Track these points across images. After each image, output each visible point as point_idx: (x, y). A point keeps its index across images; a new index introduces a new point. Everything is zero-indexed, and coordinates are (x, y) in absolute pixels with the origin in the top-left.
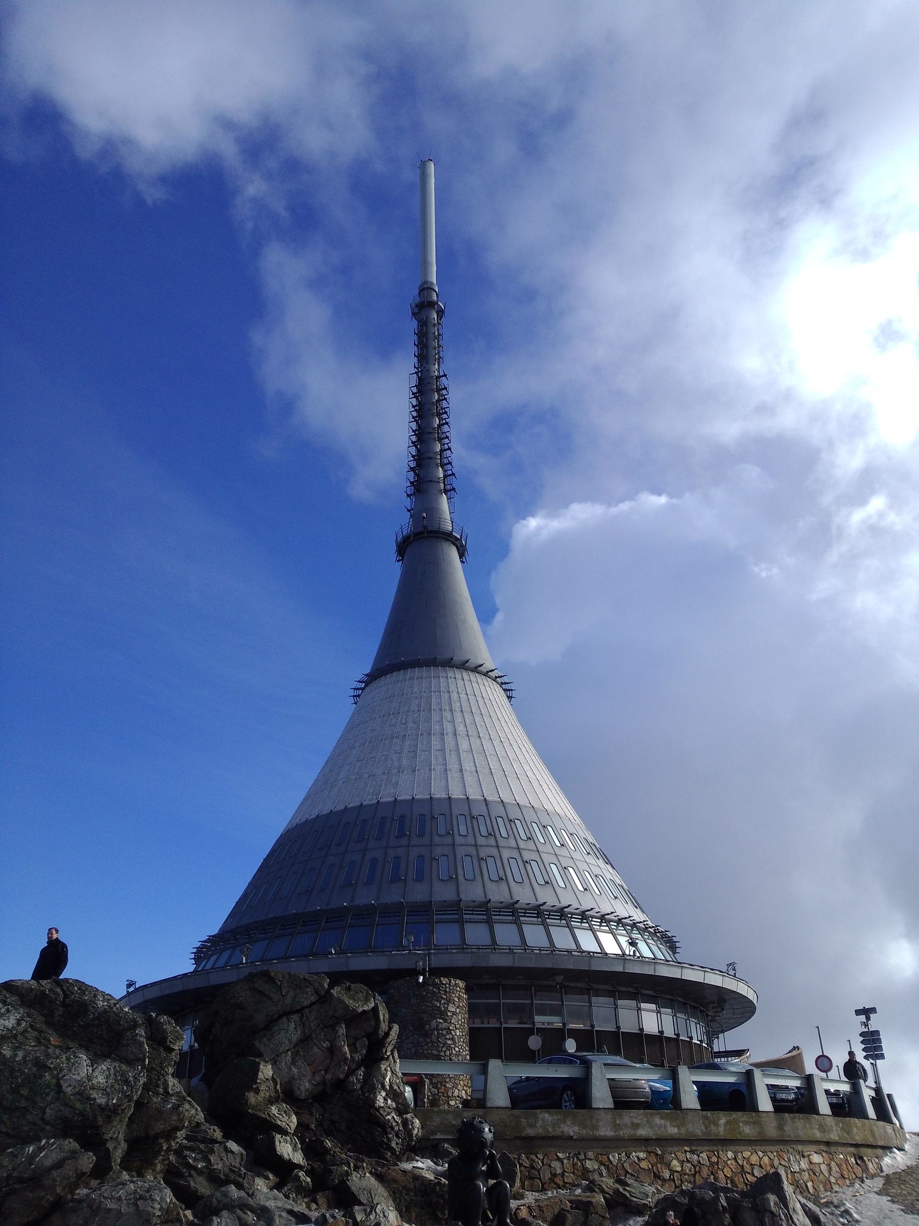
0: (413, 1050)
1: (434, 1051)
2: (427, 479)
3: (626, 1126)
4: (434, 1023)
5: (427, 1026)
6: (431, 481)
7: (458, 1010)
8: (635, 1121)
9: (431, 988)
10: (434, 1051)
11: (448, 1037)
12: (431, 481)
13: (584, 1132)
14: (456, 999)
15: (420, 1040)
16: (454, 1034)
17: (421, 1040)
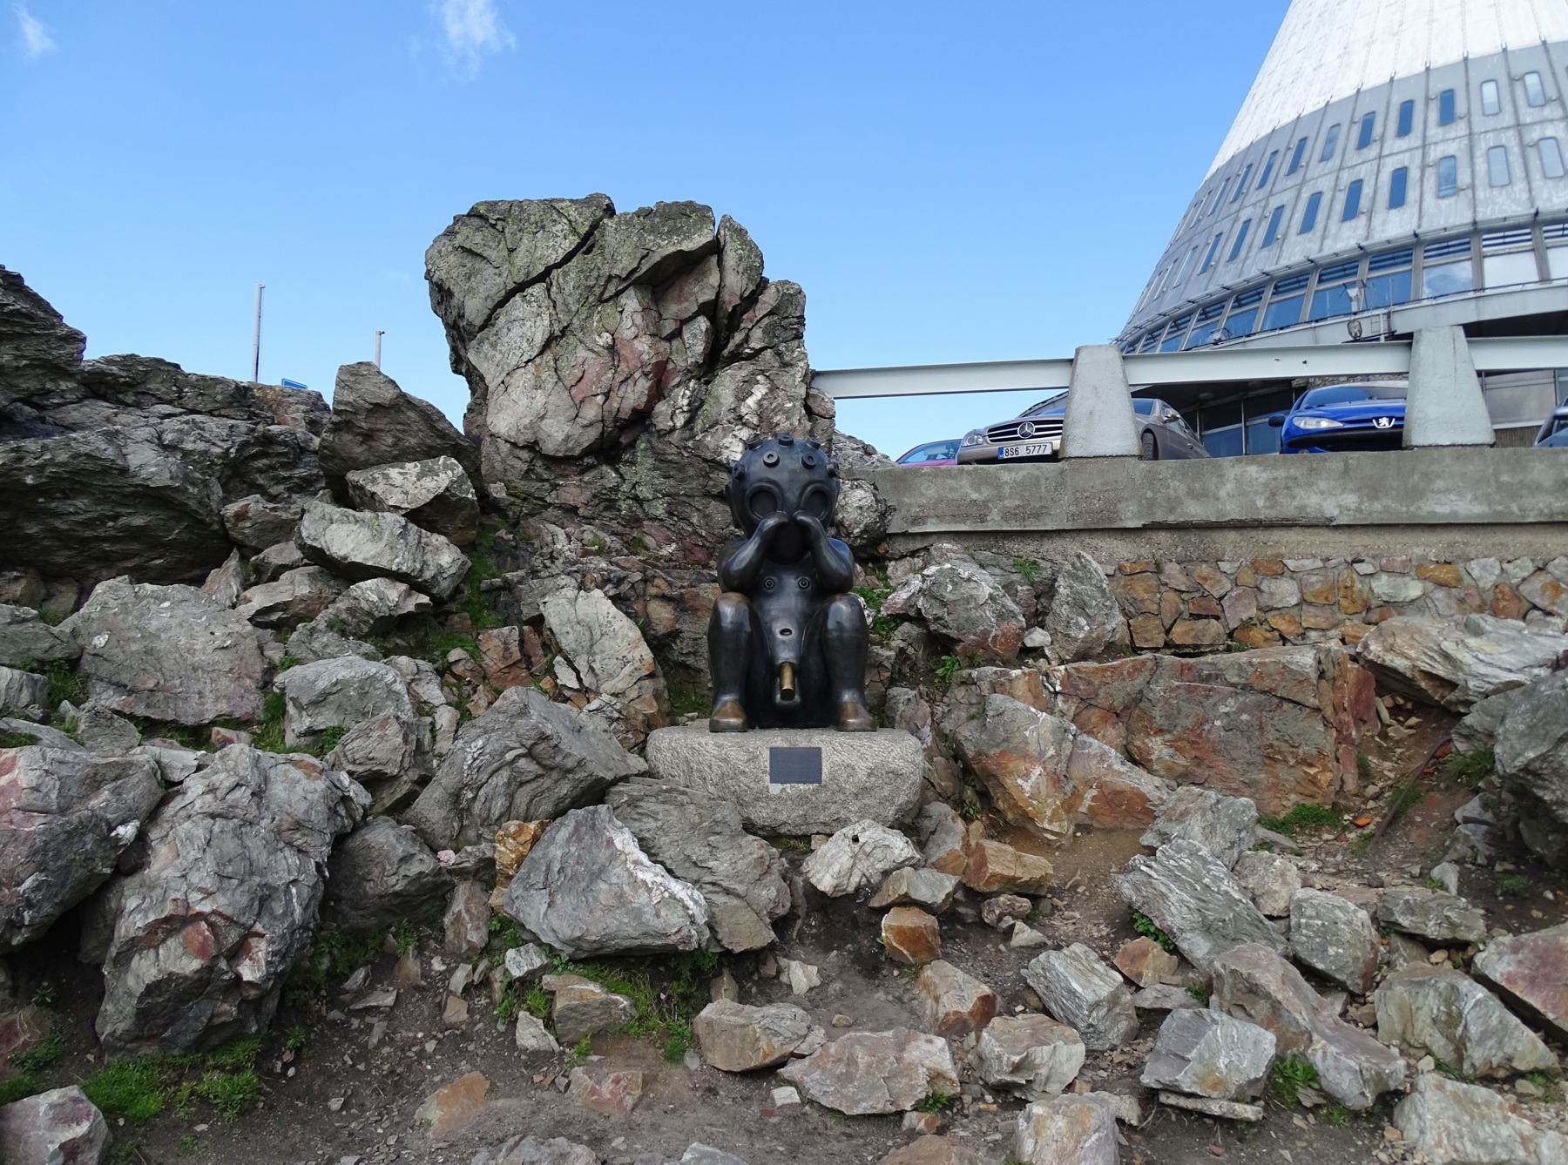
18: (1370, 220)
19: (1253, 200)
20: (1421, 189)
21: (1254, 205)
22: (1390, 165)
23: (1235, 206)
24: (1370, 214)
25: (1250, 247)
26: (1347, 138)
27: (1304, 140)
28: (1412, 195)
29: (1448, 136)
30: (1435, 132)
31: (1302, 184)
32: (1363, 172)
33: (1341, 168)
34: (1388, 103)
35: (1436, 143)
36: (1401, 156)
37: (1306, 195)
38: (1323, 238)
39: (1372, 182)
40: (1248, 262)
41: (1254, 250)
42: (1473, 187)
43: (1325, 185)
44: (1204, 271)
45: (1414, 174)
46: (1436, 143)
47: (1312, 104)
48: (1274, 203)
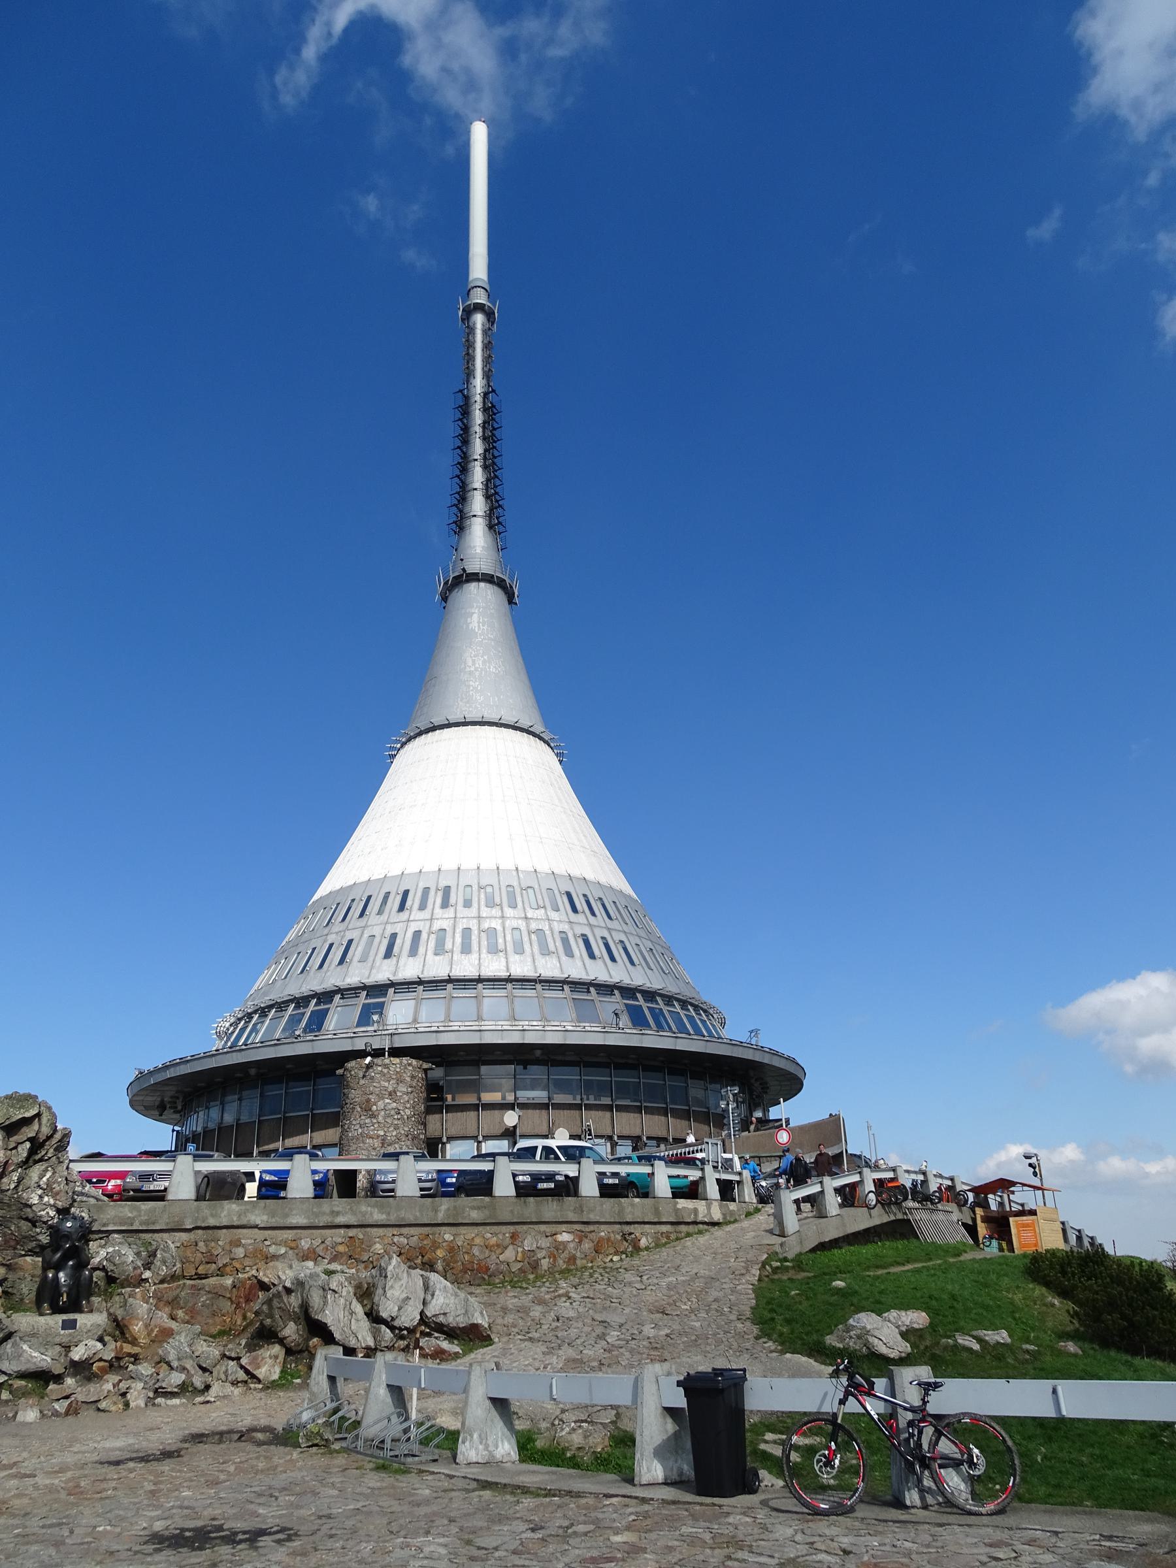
0: (360, 1130)
1: (379, 1132)
2: (472, 514)
3: (324, 1213)
4: (381, 1104)
5: (375, 1107)
6: (475, 516)
7: (409, 1089)
8: (336, 1209)
9: (380, 1068)
10: (379, 1132)
11: (396, 1117)
12: (475, 516)
13: (274, 1220)
14: (408, 1079)
15: (366, 1121)
16: (403, 1114)
17: (368, 1121)
18: (398, 962)
19: (337, 930)
20: (428, 944)
21: (337, 933)
22: (413, 927)
23: (326, 931)
24: (399, 957)
25: (331, 963)
26: (393, 903)
27: (369, 897)
28: (421, 950)
29: (444, 916)
30: (438, 911)
31: (364, 927)
32: (398, 928)
33: (387, 923)
34: (417, 886)
35: (437, 919)
36: (420, 922)
37: (366, 935)
38: (372, 967)
39: (403, 936)
40: (329, 974)
41: (333, 966)
42: (452, 952)
43: (377, 931)
44: (302, 972)
45: (424, 936)
46: (437, 919)
47: (378, 875)
48: (349, 936)
